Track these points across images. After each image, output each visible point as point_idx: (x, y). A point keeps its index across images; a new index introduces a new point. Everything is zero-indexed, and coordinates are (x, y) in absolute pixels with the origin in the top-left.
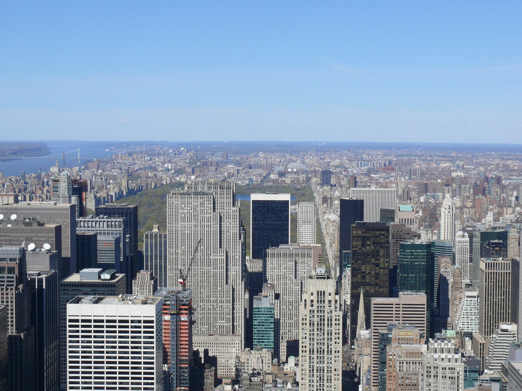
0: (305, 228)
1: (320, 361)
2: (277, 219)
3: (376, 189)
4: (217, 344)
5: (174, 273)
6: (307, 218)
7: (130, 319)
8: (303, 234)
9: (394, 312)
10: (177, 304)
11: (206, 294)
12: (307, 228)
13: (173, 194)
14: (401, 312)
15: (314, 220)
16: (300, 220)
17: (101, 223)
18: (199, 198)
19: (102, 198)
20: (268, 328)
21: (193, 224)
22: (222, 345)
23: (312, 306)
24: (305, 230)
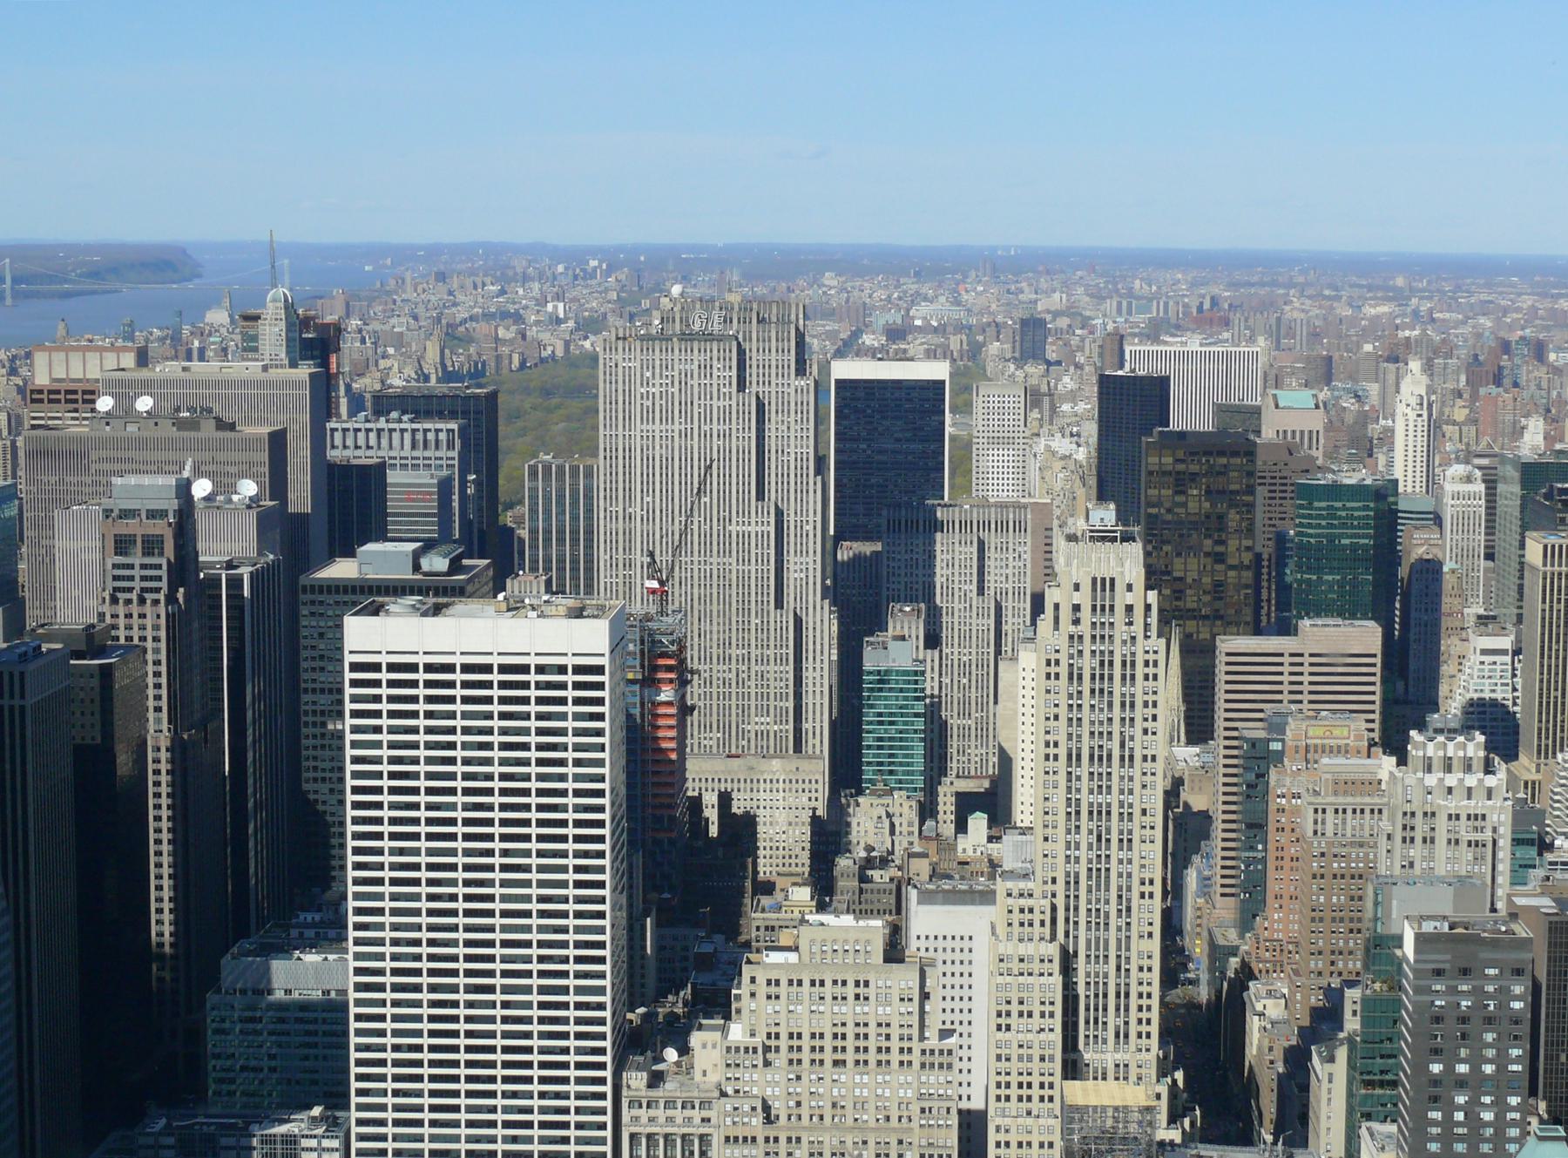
0: (996, 458)
1: (1100, 787)
2: (908, 435)
3: (1203, 349)
4: (752, 781)
5: (621, 576)
6: (1001, 429)
7: (533, 661)
8: (990, 476)
9: (1286, 678)
10: (642, 652)
11: (715, 637)
12: (1001, 458)
13: (618, 338)
14: (1306, 679)
15: (1021, 435)
16: (981, 435)
17: (396, 436)
18: (696, 351)
19: (368, 396)
20: (907, 731)
21: (676, 427)
22: (768, 785)
23: (1076, 622)
24: (996, 464)
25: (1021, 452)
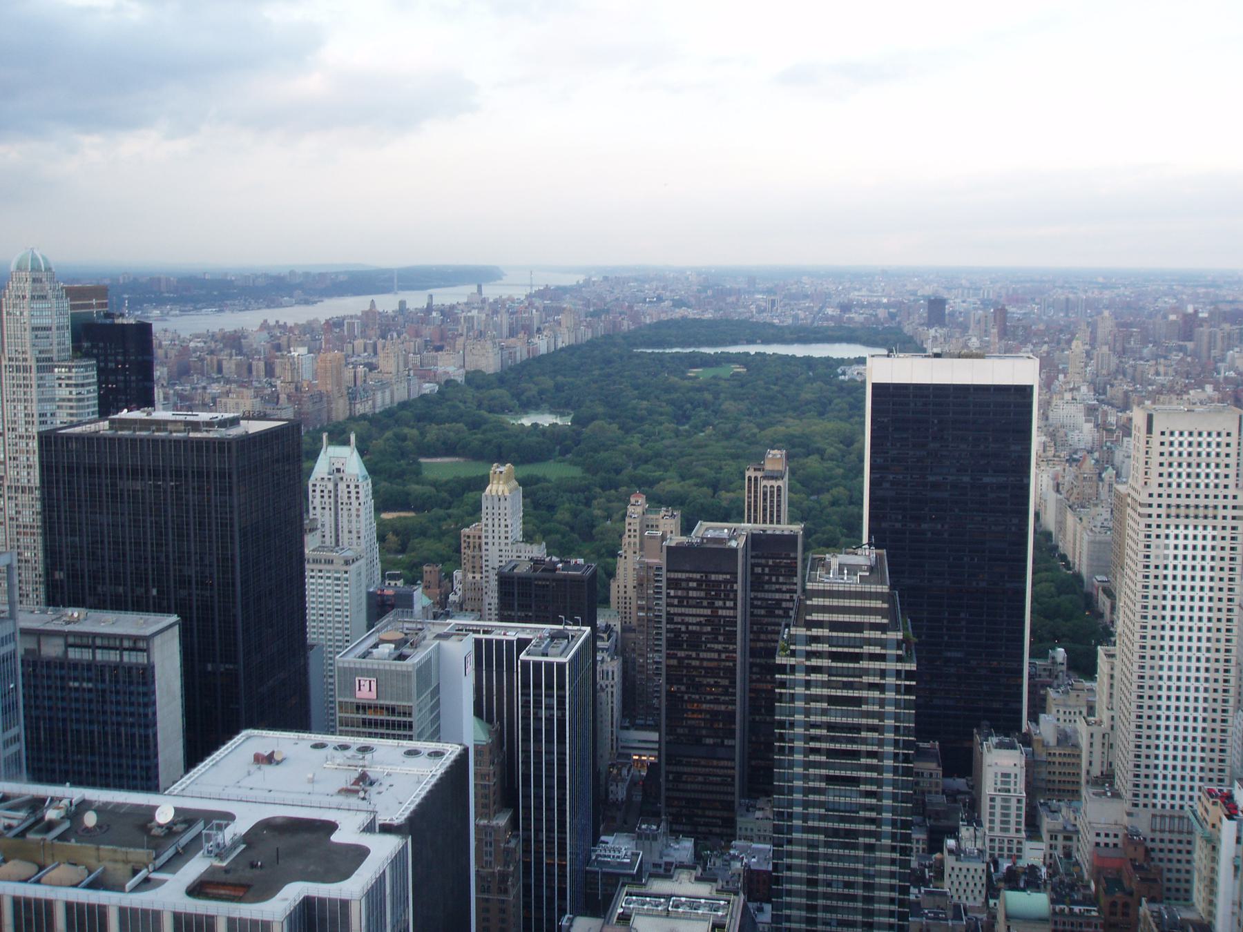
0: (1181, 542)
6: (1192, 491)
8: (1170, 572)
12: (1190, 542)
15: (1230, 502)
24: (1180, 552)
25: (1228, 533)
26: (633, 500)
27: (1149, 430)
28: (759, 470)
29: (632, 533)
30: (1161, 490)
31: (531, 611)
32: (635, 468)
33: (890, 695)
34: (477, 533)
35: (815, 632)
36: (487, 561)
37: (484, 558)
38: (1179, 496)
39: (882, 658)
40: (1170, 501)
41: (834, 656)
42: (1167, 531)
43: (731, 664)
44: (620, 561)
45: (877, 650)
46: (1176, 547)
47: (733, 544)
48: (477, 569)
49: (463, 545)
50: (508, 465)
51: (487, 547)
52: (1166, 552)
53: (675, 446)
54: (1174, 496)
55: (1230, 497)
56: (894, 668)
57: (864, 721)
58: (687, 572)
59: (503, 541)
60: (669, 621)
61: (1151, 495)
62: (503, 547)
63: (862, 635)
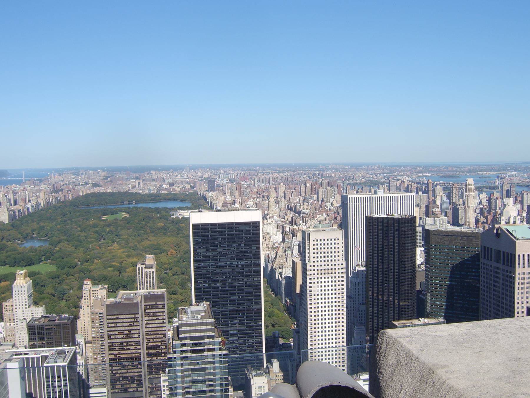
0: (323, 284)
3: (385, 195)
8: (320, 297)
15: (340, 266)
16: (312, 268)
24: (323, 288)
26: (85, 282)
27: (309, 240)
28: (143, 264)
29: (86, 298)
30: (314, 264)
31: (44, 341)
32: (82, 264)
33: (217, 365)
34: (11, 304)
35: (184, 342)
36: (16, 317)
37: (15, 315)
38: (321, 266)
39: (213, 350)
40: (318, 268)
41: (193, 352)
42: (318, 280)
43: (139, 355)
44: (81, 312)
45: (211, 347)
46: (321, 286)
47: (136, 301)
48: (12, 321)
49: (4, 310)
50: (25, 270)
51: (16, 310)
52: (318, 289)
53: (100, 253)
54: (319, 266)
55: (340, 264)
56: (218, 353)
57: (207, 377)
58: (116, 315)
59: (24, 306)
60: (109, 338)
61: (311, 266)
62: (24, 309)
63: (204, 341)
